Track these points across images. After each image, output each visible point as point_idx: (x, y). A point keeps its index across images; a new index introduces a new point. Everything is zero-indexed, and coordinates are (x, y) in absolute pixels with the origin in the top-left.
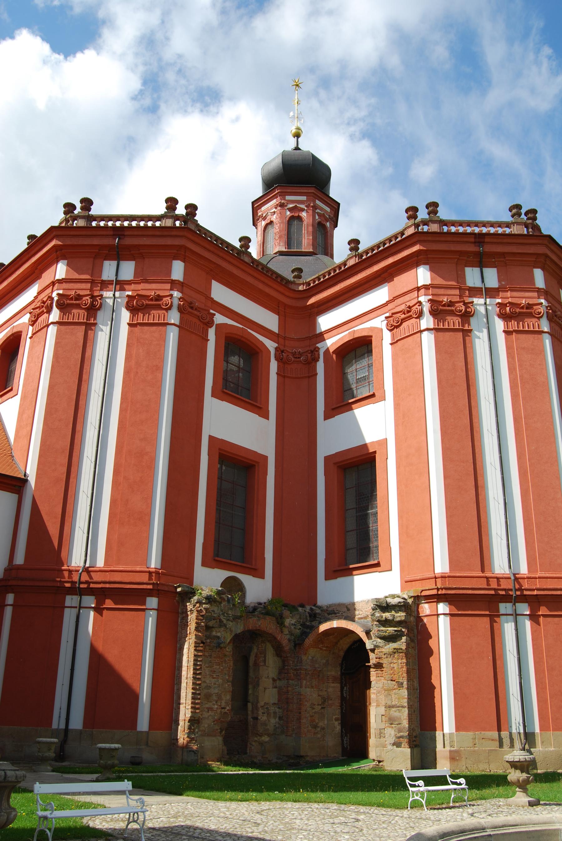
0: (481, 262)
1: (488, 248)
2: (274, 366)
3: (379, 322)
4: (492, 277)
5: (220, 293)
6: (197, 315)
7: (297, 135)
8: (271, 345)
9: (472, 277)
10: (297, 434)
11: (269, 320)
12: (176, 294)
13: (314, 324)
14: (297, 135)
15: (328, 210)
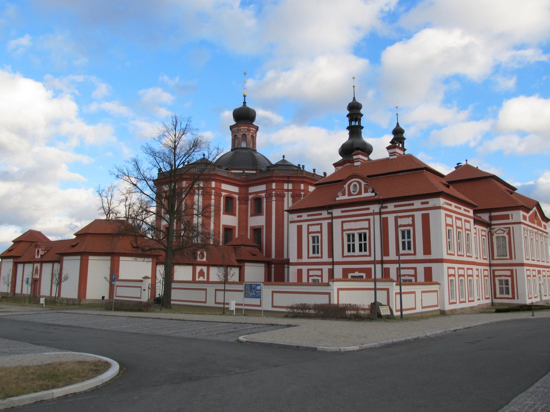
0: (288, 182)
1: (290, 179)
2: (237, 202)
3: (263, 195)
4: (290, 186)
5: (224, 187)
6: (218, 195)
7: (245, 96)
8: (237, 196)
9: (286, 186)
10: (243, 221)
11: (235, 189)
12: (213, 191)
13: (248, 190)
14: (245, 96)
15: (254, 129)
